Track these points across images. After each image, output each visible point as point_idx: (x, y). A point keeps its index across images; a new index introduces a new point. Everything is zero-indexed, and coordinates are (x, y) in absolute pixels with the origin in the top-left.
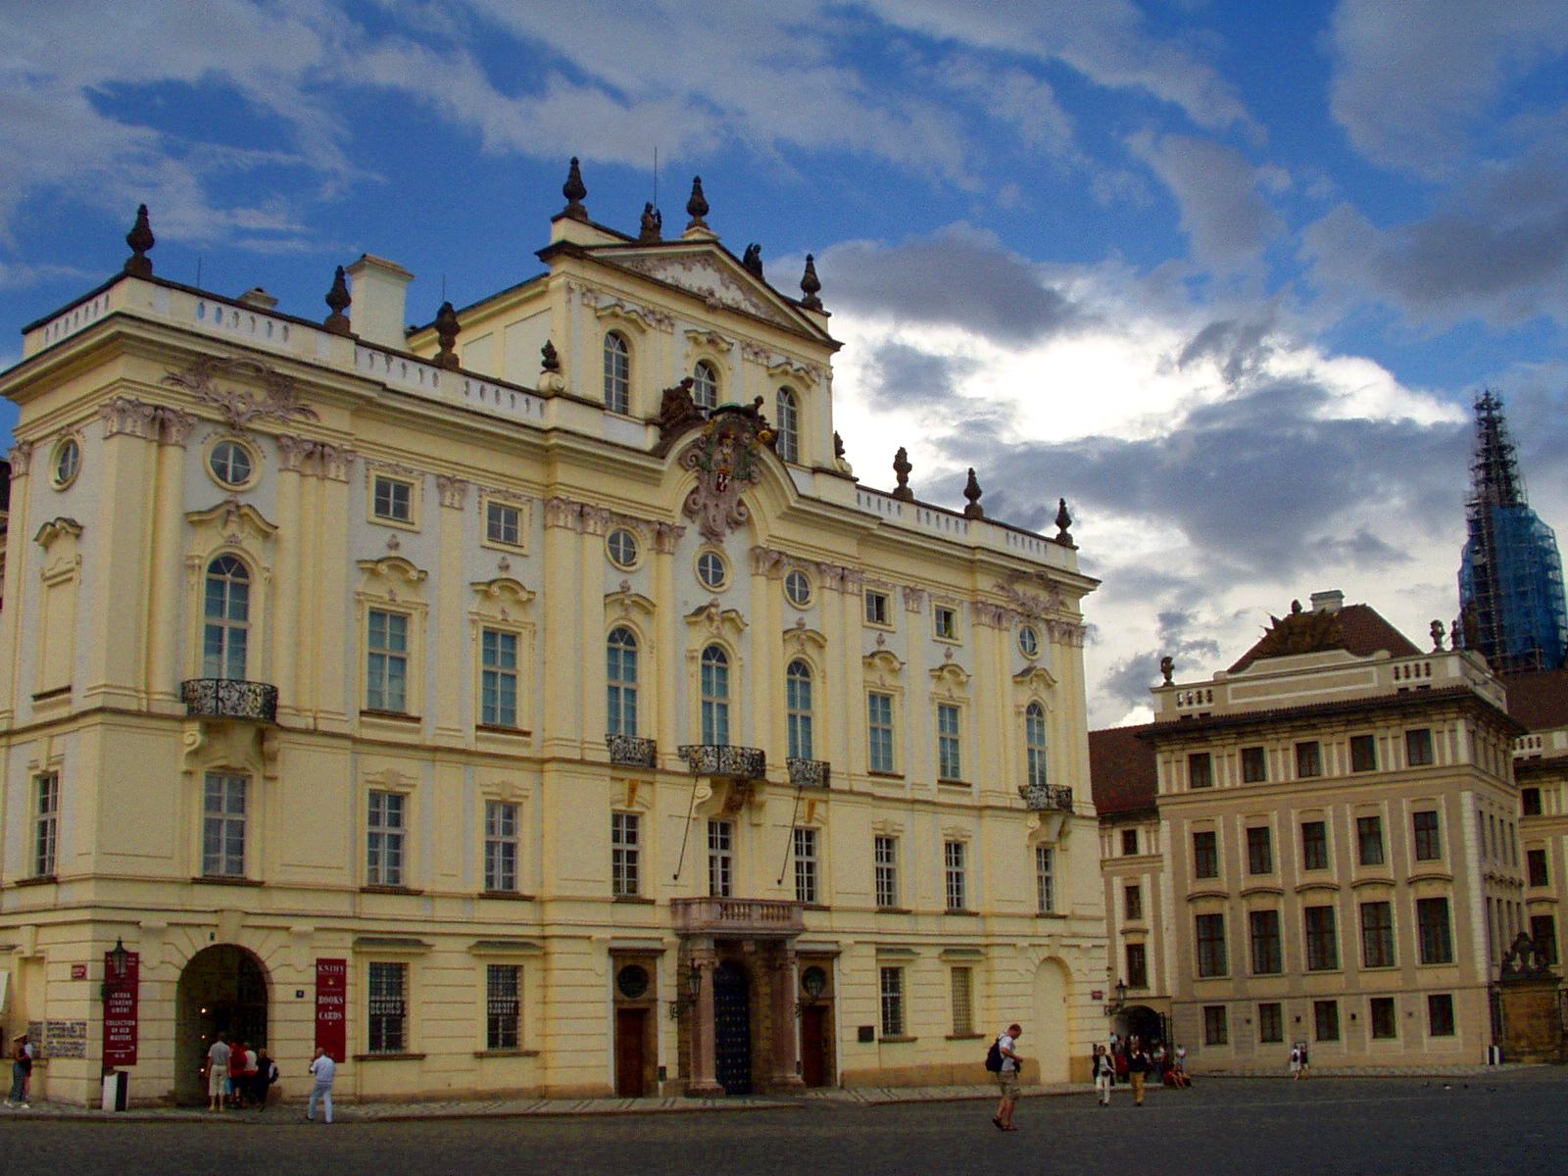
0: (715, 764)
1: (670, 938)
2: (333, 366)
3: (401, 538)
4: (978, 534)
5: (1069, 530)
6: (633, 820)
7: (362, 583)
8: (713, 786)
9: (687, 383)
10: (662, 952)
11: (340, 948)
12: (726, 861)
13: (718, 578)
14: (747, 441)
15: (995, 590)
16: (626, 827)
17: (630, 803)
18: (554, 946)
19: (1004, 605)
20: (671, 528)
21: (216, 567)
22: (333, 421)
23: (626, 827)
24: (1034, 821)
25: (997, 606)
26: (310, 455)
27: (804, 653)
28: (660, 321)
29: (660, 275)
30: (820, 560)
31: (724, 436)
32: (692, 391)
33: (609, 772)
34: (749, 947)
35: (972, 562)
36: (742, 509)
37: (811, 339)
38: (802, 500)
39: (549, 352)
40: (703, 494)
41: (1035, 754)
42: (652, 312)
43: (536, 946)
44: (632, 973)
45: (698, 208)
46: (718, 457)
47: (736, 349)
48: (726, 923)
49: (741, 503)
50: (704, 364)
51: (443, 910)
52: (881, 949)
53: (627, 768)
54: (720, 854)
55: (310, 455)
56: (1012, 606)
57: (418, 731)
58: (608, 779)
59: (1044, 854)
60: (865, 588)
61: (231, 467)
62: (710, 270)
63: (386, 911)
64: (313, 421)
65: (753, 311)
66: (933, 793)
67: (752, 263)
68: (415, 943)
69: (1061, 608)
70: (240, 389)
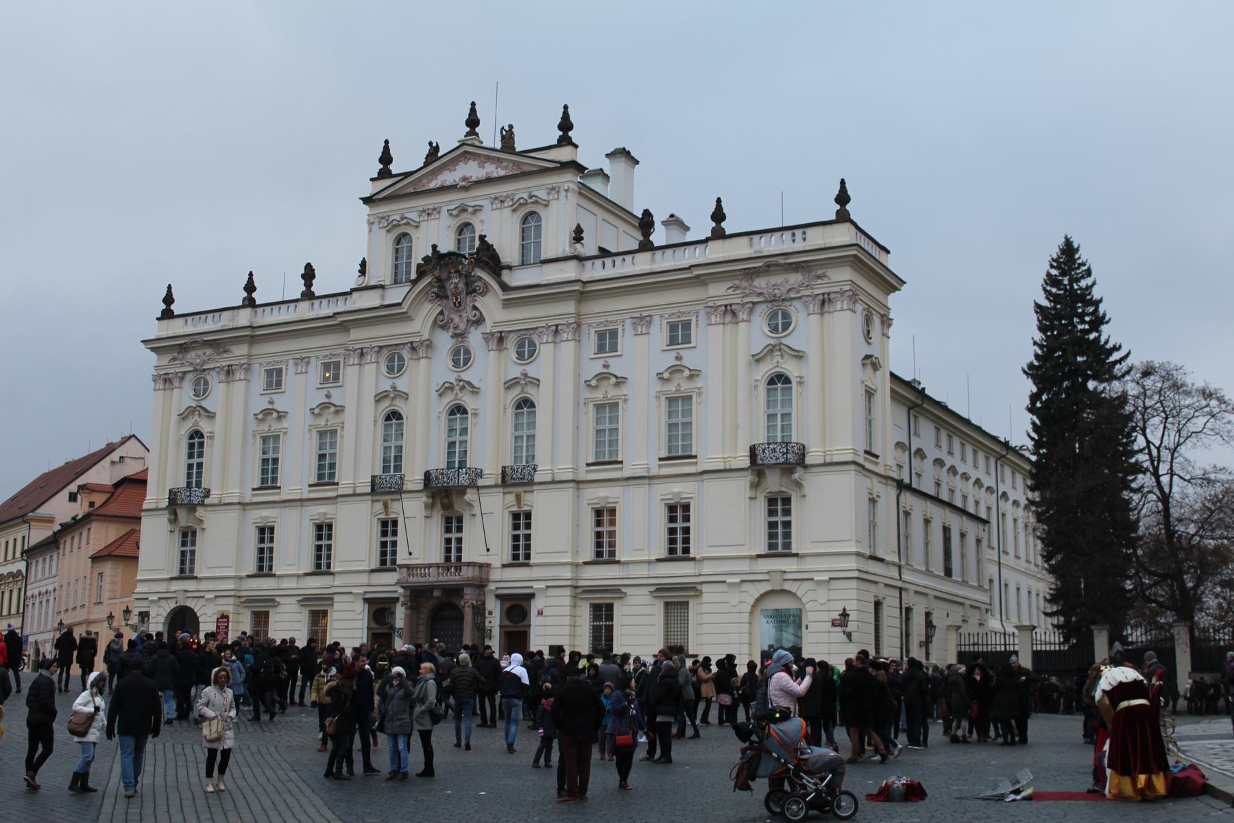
1: (401, 590)
4: (717, 251)
5: (848, 207)
6: (395, 523)
7: (253, 425)
8: (433, 496)
9: (434, 247)
10: (397, 599)
11: (228, 606)
12: (459, 540)
13: (466, 361)
15: (730, 292)
16: (388, 527)
17: (387, 514)
18: (336, 598)
19: (738, 301)
20: (422, 343)
21: (191, 437)
22: (240, 350)
23: (388, 527)
24: (748, 478)
26: (228, 372)
28: (429, 214)
29: (432, 185)
32: (447, 246)
33: (369, 498)
34: (436, 593)
35: (698, 277)
37: (546, 171)
39: (363, 264)
40: (446, 313)
41: (779, 418)
42: (424, 211)
43: (329, 599)
44: (380, 610)
45: (473, 122)
46: (450, 286)
47: (486, 203)
48: (411, 579)
49: (475, 308)
50: (464, 227)
51: (286, 584)
52: (579, 592)
53: (378, 494)
54: (453, 536)
56: (746, 300)
59: (779, 505)
61: (202, 388)
62: (471, 162)
63: (263, 585)
65: (502, 173)
67: (508, 137)
68: (271, 601)
69: (820, 281)
70: (200, 352)
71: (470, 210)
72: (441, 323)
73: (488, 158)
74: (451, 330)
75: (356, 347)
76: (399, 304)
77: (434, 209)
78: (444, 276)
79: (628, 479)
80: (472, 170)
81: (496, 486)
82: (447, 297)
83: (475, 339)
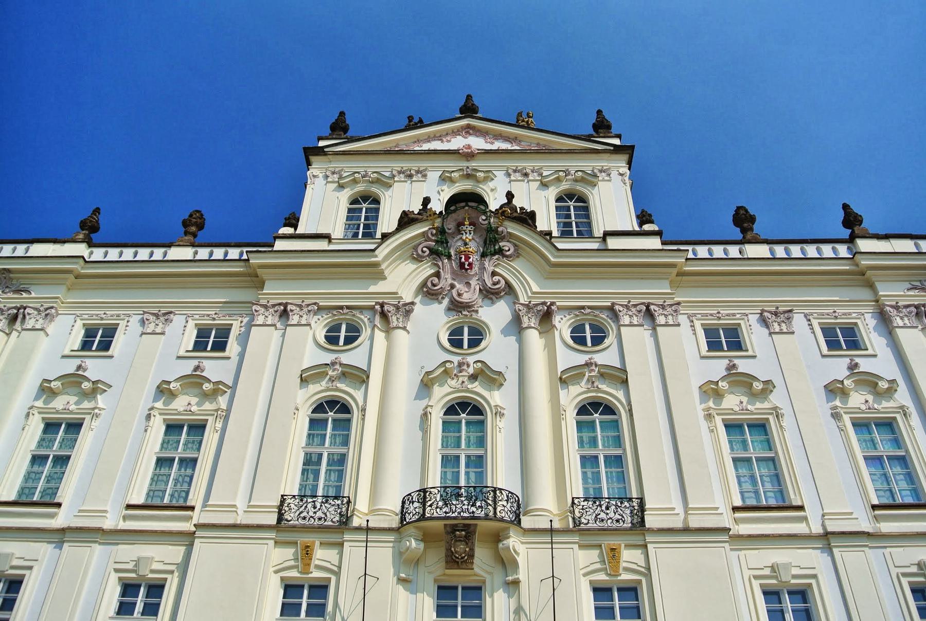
0: (421, 511)
2: (49, 255)
3: (89, 363)
9: (426, 201)
14: (486, 222)
25: (917, 307)
27: (599, 390)
28: (411, 176)
30: (609, 304)
31: (460, 224)
33: (273, 535)
36: (496, 278)
38: (561, 253)
49: (494, 274)
55: (13, 319)
57: (52, 516)
58: (272, 542)
60: (698, 324)
64: (25, 295)
66: (865, 524)
71: (481, 175)
72: (429, 292)
73: (499, 136)
74: (446, 302)
75: (272, 302)
76: (373, 251)
77: (418, 172)
78: (450, 226)
79: (827, 535)
80: (477, 143)
81: (565, 531)
82: (449, 257)
83: (494, 315)
